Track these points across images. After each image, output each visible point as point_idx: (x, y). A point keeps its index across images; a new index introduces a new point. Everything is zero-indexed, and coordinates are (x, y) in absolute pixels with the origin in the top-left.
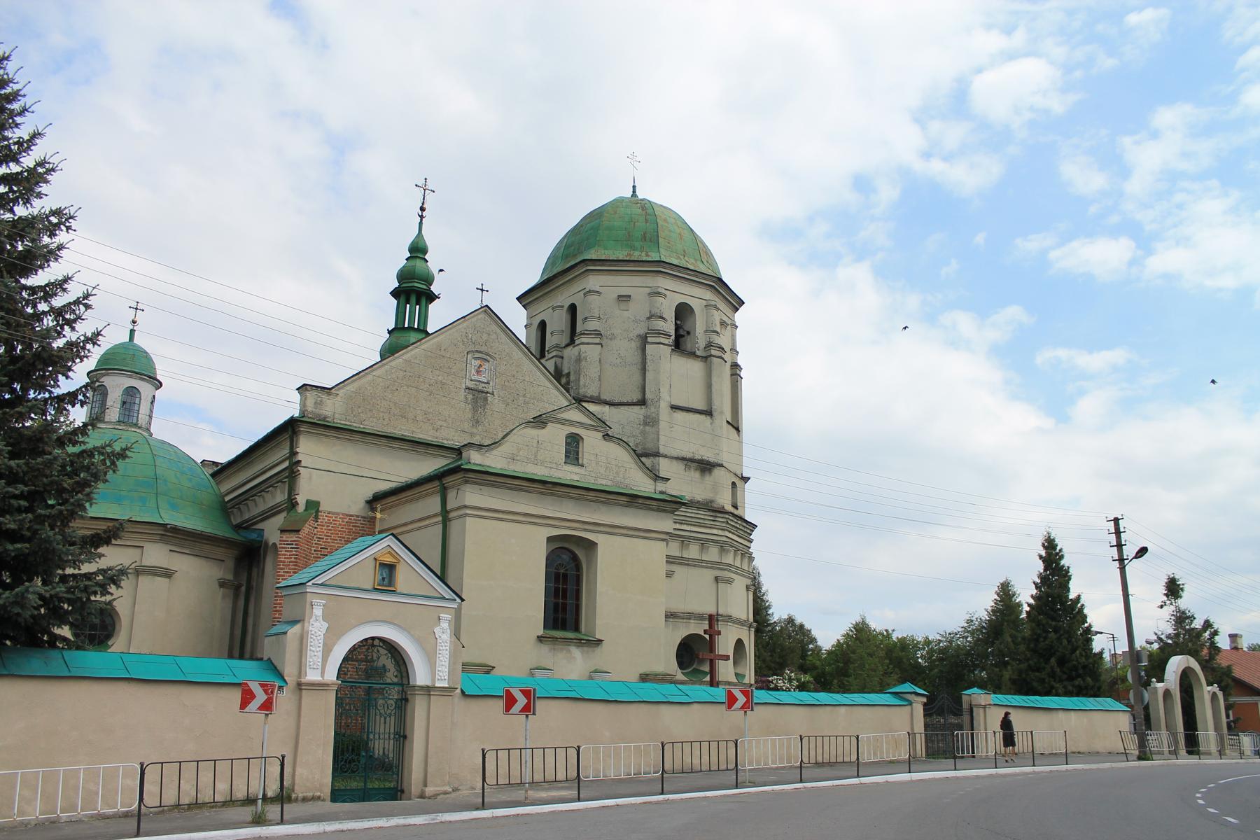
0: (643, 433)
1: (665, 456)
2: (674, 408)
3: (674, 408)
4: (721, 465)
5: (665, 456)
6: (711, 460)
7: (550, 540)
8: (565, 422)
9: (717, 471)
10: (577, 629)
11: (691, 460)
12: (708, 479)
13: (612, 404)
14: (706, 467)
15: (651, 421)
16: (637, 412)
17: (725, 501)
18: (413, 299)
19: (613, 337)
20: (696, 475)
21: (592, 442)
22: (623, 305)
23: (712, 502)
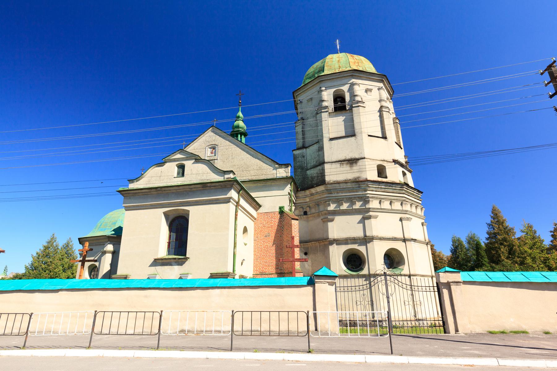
0: (319, 155)
1: (329, 162)
2: (331, 139)
3: (331, 139)
4: (364, 158)
5: (329, 162)
6: (357, 157)
7: (166, 214)
8: (175, 160)
9: (360, 162)
10: (185, 255)
11: (344, 161)
12: (355, 168)
13: (306, 148)
14: (352, 162)
15: (321, 149)
16: (316, 147)
17: (373, 175)
18: (239, 136)
19: (308, 118)
20: (348, 166)
21: (189, 164)
22: (310, 103)
23: (358, 178)
